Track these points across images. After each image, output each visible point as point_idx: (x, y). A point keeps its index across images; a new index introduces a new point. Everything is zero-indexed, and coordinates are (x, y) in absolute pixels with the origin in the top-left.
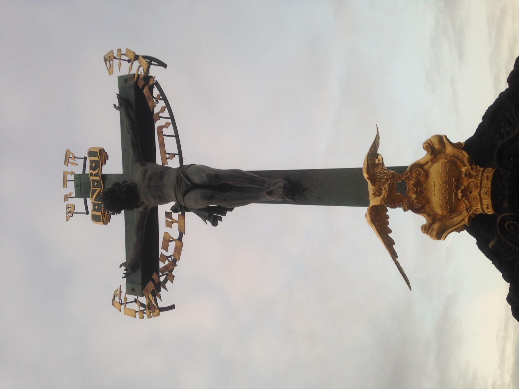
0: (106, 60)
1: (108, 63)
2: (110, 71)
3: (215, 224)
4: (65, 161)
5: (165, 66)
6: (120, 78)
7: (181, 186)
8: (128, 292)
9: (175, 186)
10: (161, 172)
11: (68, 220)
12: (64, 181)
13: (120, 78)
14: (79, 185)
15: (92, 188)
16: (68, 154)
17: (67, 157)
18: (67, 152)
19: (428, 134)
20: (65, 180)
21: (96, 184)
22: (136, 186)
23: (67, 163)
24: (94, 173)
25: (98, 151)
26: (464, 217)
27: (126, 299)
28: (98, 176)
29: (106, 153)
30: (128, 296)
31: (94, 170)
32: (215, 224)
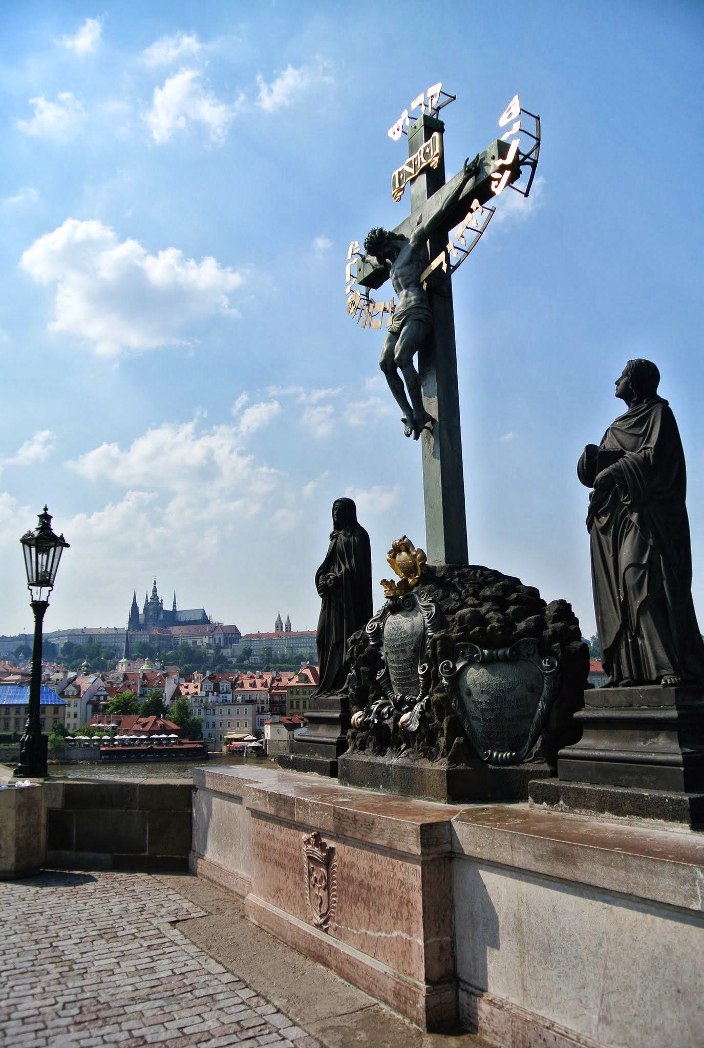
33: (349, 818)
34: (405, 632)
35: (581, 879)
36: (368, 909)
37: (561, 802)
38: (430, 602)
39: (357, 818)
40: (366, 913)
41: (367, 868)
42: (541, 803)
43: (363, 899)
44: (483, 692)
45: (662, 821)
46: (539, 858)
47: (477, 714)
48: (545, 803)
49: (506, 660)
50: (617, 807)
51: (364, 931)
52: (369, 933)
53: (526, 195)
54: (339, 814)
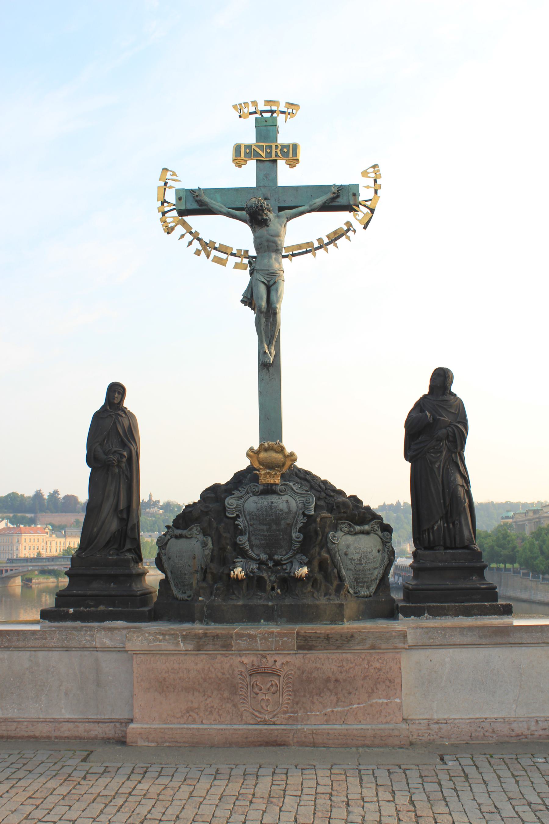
0: (375, 166)
1: (372, 170)
2: (365, 174)
3: (242, 301)
4: (289, 104)
5: (365, 228)
6: (357, 186)
7: (268, 276)
8: (177, 191)
9: (268, 270)
10: (278, 250)
11: (235, 107)
12: (270, 101)
13: (357, 186)
14: (267, 124)
15: (264, 145)
16: (296, 107)
17: (293, 107)
18: (298, 106)
19: (297, 453)
20: (271, 103)
21: (268, 151)
22: (268, 226)
23: (288, 105)
24: (278, 151)
25: (297, 158)
26: (256, 465)
27: (171, 187)
28: (276, 156)
29: (295, 166)
30: (173, 190)
31: (280, 150)
32: (242, 301)
33: (319, 637)
34: (281, 510)
35: (513, 642)
36: (336, 694)
37: (426, 615)
38: (306, 491)
39: (330, 636)
40: (334, 698)
41: (335, 669)
42: (410, 617)
43: (328, 689)
44: (356, 553)
45: (496, 616)
46: (480, 637)
47: (351, 567)
48: (412, 617)
49: (367, 533)
50: (468, 613)
51: (329, 710)
52: (335, 710)
53: (365, 228)
54: (304, 637)
